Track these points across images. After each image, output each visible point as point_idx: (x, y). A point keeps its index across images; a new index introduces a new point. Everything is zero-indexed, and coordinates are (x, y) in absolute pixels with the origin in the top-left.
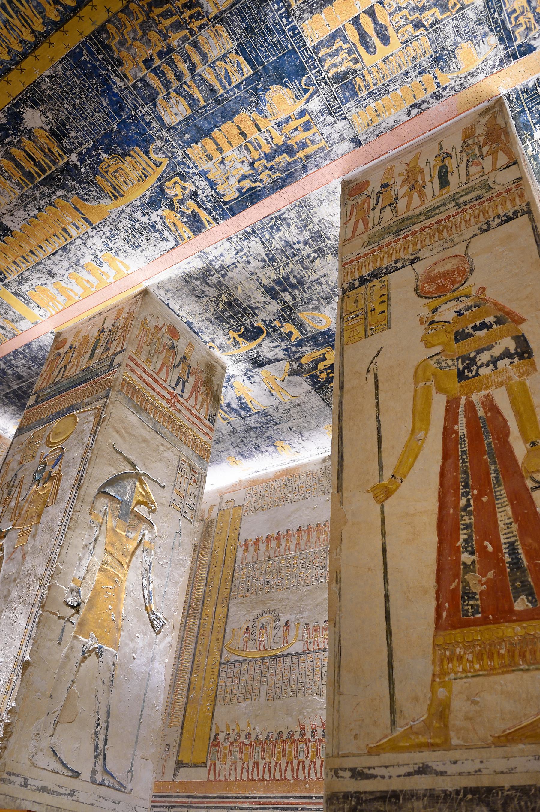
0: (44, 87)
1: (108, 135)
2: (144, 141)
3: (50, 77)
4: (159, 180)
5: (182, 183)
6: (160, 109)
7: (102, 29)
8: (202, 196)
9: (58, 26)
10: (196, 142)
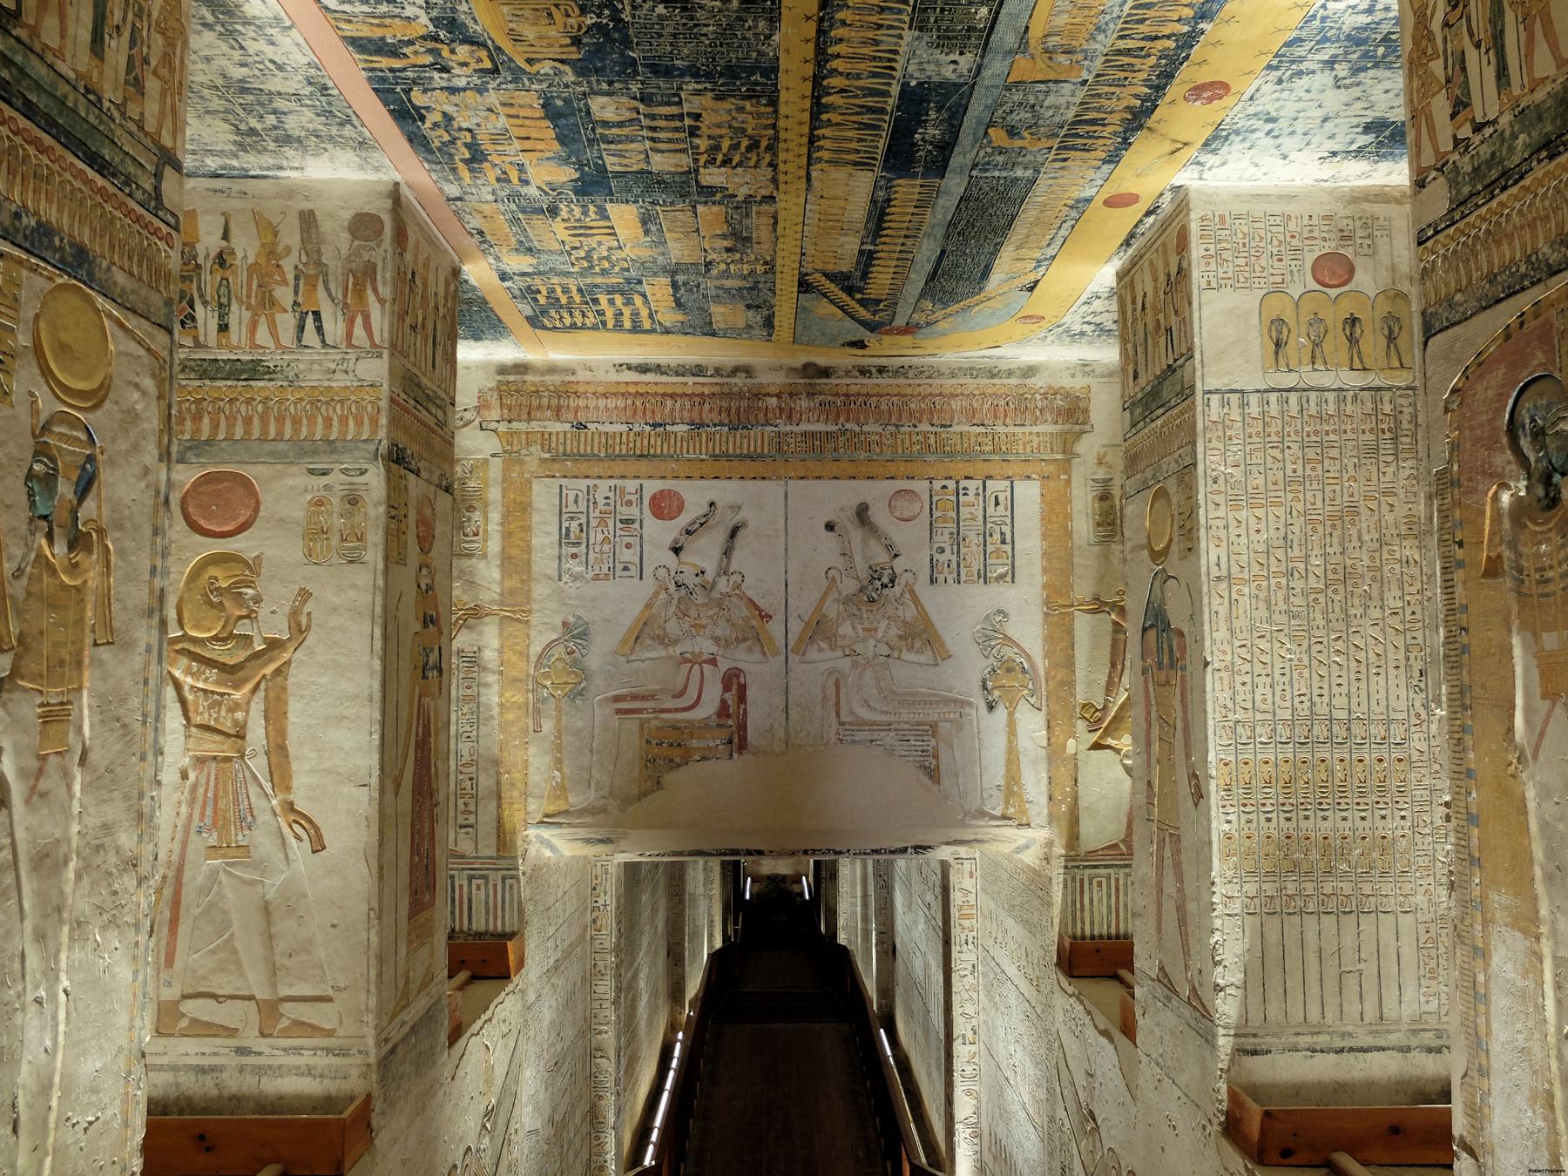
0: (762, 24)
1: (626, 42)
2: (582, 69)
3: (768, 37)
4: (498, 49)
5: (474, 65)
6: (624, 100)
7: (774, 103)
8: (436, 75)
9: (817, 80)
10: (543, 106)
